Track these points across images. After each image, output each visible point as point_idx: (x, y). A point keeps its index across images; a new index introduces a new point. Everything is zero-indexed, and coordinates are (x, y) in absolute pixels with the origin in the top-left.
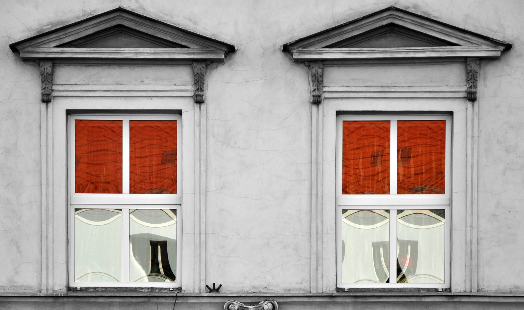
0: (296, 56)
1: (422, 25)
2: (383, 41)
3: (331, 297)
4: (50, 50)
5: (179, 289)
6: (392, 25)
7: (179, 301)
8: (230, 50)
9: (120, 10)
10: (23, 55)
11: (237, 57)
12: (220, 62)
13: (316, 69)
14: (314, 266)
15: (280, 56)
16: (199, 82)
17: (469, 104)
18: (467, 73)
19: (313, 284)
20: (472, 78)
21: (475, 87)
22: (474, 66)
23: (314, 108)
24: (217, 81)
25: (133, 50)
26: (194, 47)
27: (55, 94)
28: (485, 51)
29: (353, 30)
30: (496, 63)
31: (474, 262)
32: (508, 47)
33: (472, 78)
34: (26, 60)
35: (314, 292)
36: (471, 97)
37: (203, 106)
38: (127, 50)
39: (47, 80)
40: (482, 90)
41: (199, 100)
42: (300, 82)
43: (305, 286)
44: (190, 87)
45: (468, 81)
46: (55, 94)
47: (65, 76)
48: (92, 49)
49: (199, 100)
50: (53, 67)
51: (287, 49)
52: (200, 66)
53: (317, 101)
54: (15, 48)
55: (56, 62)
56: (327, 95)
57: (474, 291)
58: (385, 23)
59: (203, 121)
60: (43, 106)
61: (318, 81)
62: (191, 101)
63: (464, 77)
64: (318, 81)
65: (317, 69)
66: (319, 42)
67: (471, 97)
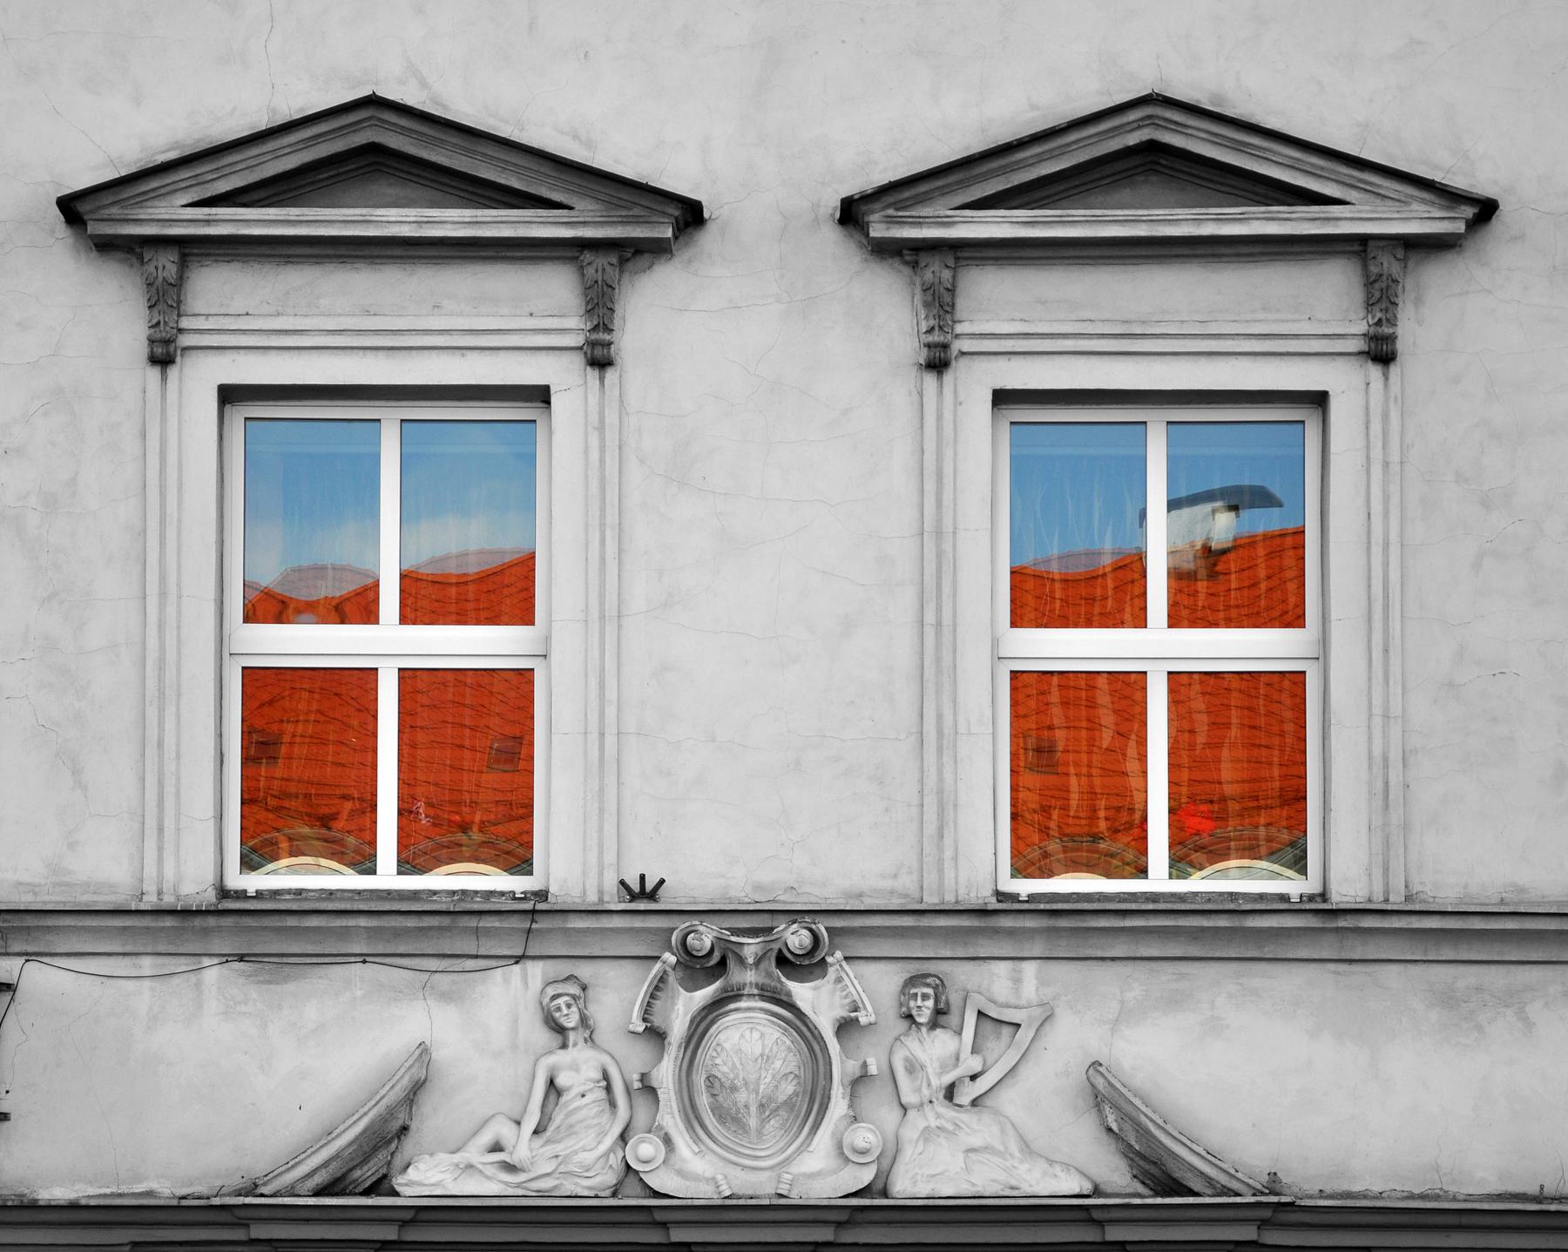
0: (878, 231)
1: (1239, 147)
2: (1126, 194)
3: (983, 912)
4: (172, 213)
5: (542, 895)
6: (1152, 147)
7: (542, 924)
8: (690, 215)
9: (373, 101)
10: (94, 228)
11: (707, 239)
12: (657, 250)
13: (934, 268)
14: (931, 828)
15: (832, 237)
16: (600, 307)
17: (1375, 371)
18: (1369, 283)
19: (930, 879)
20: (1381, 297)
21: (1392, 322)
22: (1387, 263)
23: (930, 379)
24: (652, 305)
25: (412, 213)
26: (584, 207)
27: (186, 340)
28: (1420, 219)
29: (1040, 159)
30: (1450, 256)
31: (1395, 818)
32: (1486, 210)
33: (1381, 297)
34: (106, 246)
35: (931, 901)
36: (1381, 352)
37: (611, 375)
38: (393, 213)
39: (165, 300)
40: (1409, 331)
41: (599, 359)
42: (888, 308)
43: (907, 883)
44: (574, 322)
45: (1369, 305)
46: (186, 340)
47: (217, 292)
48: (293, 212)
49: (599, 359)
50: (183, 264)
51: (851, 213)
52: (600, 263)
53: (937, 363)
54: (72, 208)
55: (192, 249)
56: (966, 345)
57: (1397, 901)
58: (1132, 139)
59: (612, 417)
60: (154, 373)
61: (941, 304)
62: (578, 360)
63: (1358, 295)
64: (941, 304)
65: (936, 270)
66: (944, 192)
67: (1381, 352)
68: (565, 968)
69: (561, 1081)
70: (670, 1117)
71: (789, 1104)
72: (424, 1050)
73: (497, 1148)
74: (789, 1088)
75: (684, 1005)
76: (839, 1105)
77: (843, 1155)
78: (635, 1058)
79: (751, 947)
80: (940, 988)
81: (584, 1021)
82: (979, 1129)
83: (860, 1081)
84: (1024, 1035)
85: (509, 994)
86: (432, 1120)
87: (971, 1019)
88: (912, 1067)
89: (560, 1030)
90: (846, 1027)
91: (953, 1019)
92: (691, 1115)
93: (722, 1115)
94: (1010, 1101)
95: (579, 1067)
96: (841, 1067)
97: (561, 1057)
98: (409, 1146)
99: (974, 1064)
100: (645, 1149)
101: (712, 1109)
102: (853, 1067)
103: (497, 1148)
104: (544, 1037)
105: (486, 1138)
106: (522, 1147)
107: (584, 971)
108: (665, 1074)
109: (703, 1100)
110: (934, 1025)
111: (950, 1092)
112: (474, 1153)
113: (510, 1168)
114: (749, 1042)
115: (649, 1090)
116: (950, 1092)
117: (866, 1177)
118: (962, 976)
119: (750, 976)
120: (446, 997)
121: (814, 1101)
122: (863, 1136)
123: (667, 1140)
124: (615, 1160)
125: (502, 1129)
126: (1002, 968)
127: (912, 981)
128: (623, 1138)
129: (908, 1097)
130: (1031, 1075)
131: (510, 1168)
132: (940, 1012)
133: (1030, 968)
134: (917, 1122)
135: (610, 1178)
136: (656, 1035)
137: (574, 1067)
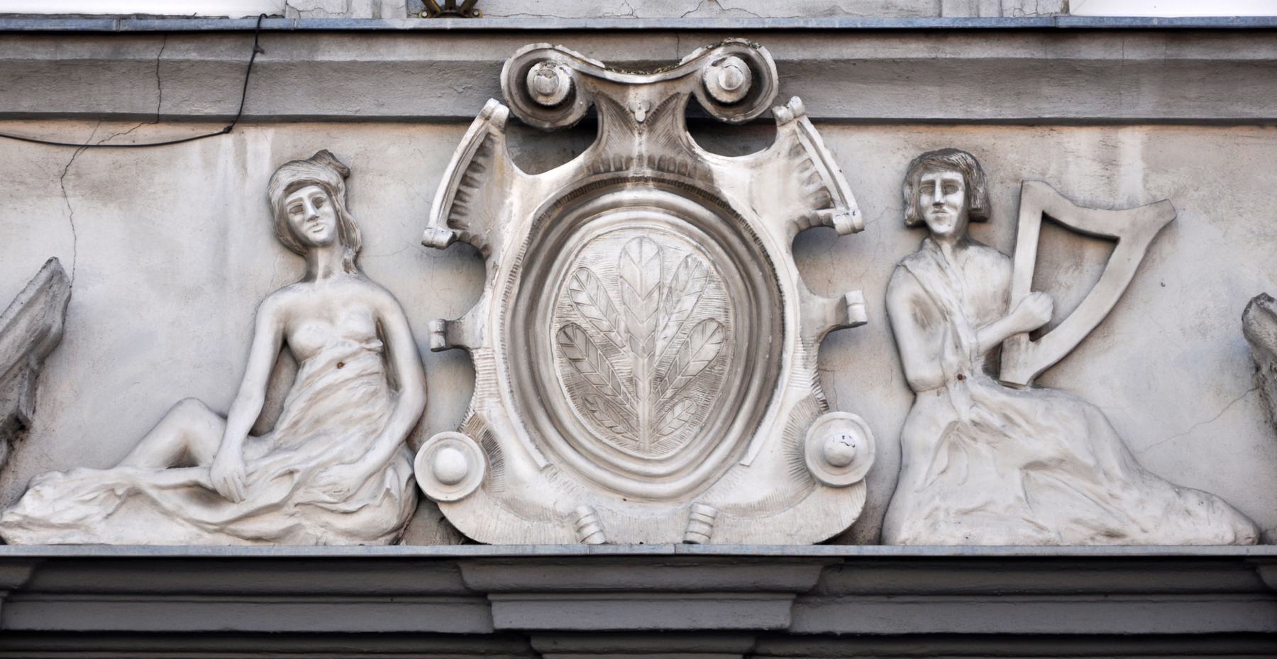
68: (311, 139)
69: (302, 339)
70: (495, 402)
71: (708, 377)
72: (54, 277)
73: (184, 459)
74: (707, 348)
75: (522, 196)
76: (797, 380)
77: (804, 472)
78: (431, 297)
79: (641, 95)
80: (973, 173)
81: (344, 231)
82: (1047, 427)
83: (836, 336)
84: (1126, 258)
85: (219, 182)
86: (72, 407)
87: (1030, 229)
88: (927, 315)
89: (299, 248)
90: (812, 238)
91: (998, 230)
92: (533, 398)
93: (591, 397)
94: (1099, 376)
95: (332, 312)
96: (804, 310)
97: (302, 296)
98: (29, 454)
99: (1036, 309)
100: (449, 458)
101: (572, 391)
102: (823, 309)
103: (184, 459)
104: (271, 261)
105: (165, 441)
106: (228, 458)
107: (347, 144)
108: (487, 324)
109: (555, 371)
110: (963, 239)
111: (994, 361)
112: (144, 470)
113: (208, 495)
114: (638, 262)
115: (457, 353)
116: (994, 361)
117: (847, 511)
118: (1012, 153)
119: (639, 145)
120: (103, 191)
121: (750, 375)
122: (840, 435)
123: (490, 446)
124: (396, 482)
125: (196, 427)
126: (1083, 140)
127: (925, 161)
128: (411, 441)
129: (920, 369)
130: (1134, 331)
131: (208, 495)
132: (975, 218)
133: (1131, 141)
134: (935, 414)
135: (386, 515)
136: (469, 253)
137: (326, 314)
